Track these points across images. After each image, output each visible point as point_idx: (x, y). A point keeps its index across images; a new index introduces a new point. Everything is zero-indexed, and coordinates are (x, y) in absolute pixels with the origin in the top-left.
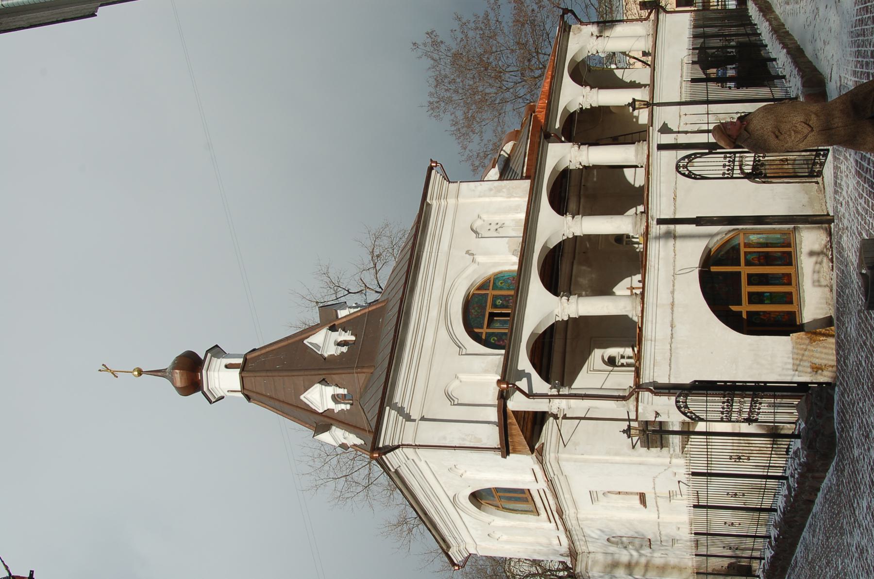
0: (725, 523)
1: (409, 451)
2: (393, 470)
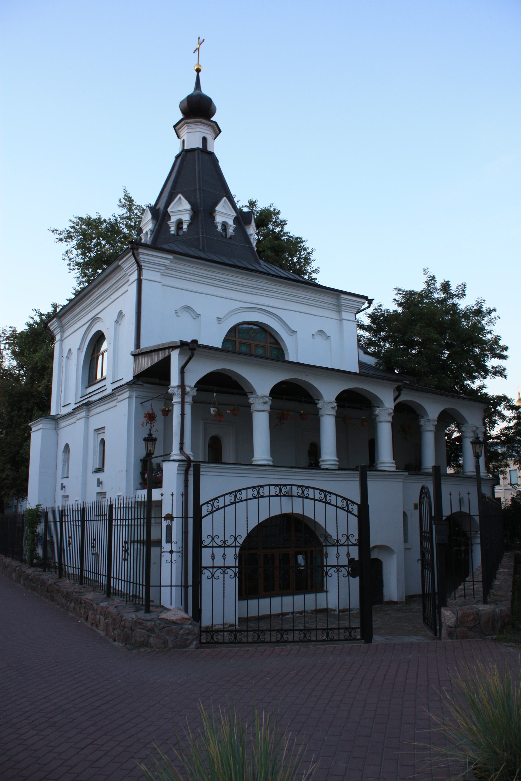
0: (70, 538)
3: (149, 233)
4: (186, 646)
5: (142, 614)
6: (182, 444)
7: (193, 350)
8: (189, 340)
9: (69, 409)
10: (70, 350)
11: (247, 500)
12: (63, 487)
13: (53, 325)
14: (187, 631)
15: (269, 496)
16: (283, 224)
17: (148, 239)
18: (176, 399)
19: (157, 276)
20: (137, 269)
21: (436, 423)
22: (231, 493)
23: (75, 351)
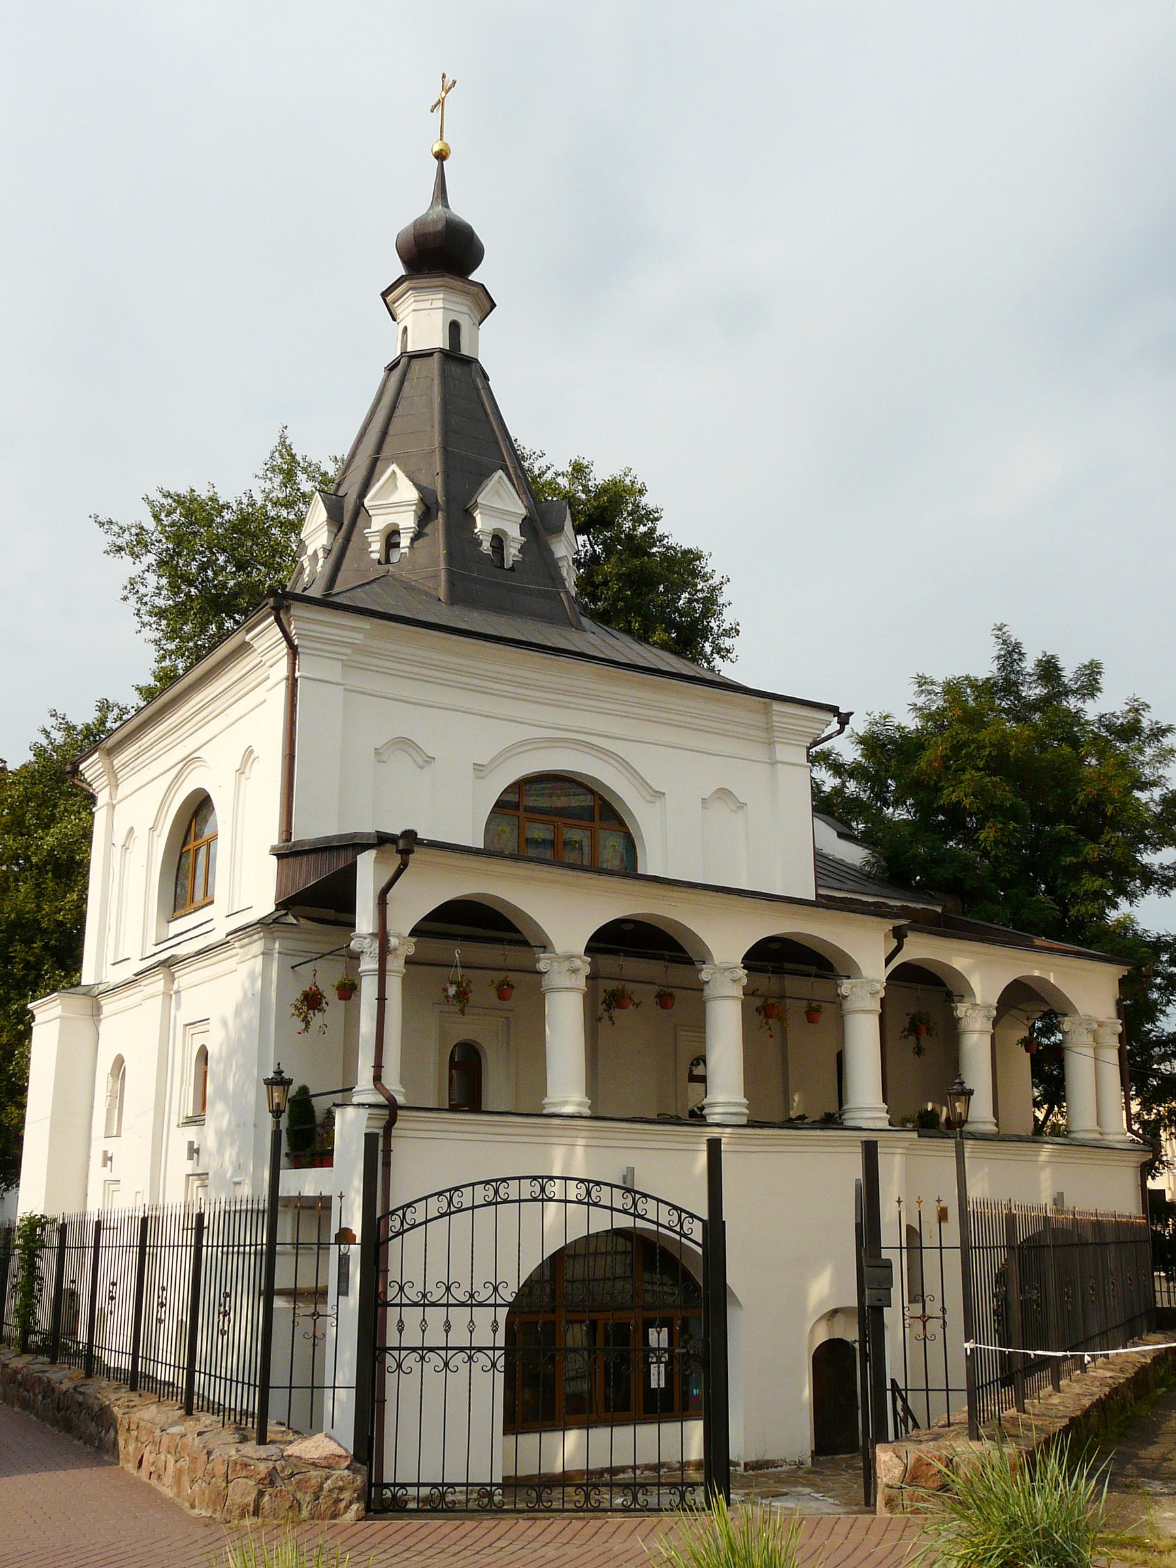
0: (114, 1284)
1: (282, 669)
2: (248, 638)
3: (321, 554)
4: (334, 1516)
5: (251, 1449)
6: (378, 1067)
7: (405, 853)
8: (398, 831)
9: (126, 972)
10: (132, 829)
11: (473, 1208)
12: (107, 1159)
13: (92, 769)
14: (341, 1483)
15: (520, 1201)
16: (650, 516)
17: (319, 569)
18: (368, 964)
19: (333, 671)
20: (287, 654)
21: (995, 1012)
22: (440, 1194)
23: (142, 833)
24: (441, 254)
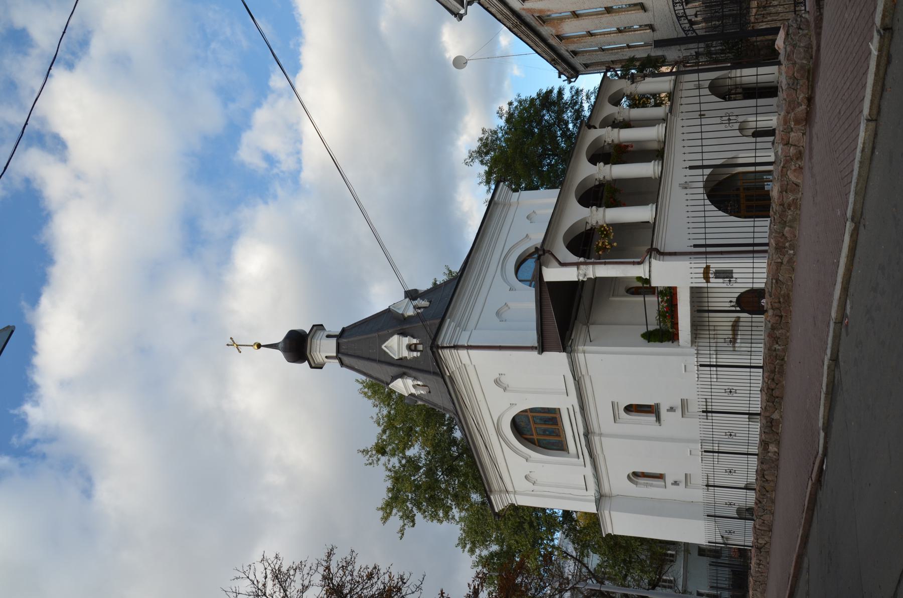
1: (463, 353)
6: (634, 263)
12: (676, 483)
24: (297, 346)
